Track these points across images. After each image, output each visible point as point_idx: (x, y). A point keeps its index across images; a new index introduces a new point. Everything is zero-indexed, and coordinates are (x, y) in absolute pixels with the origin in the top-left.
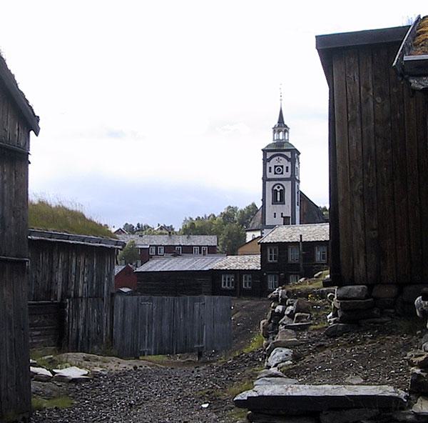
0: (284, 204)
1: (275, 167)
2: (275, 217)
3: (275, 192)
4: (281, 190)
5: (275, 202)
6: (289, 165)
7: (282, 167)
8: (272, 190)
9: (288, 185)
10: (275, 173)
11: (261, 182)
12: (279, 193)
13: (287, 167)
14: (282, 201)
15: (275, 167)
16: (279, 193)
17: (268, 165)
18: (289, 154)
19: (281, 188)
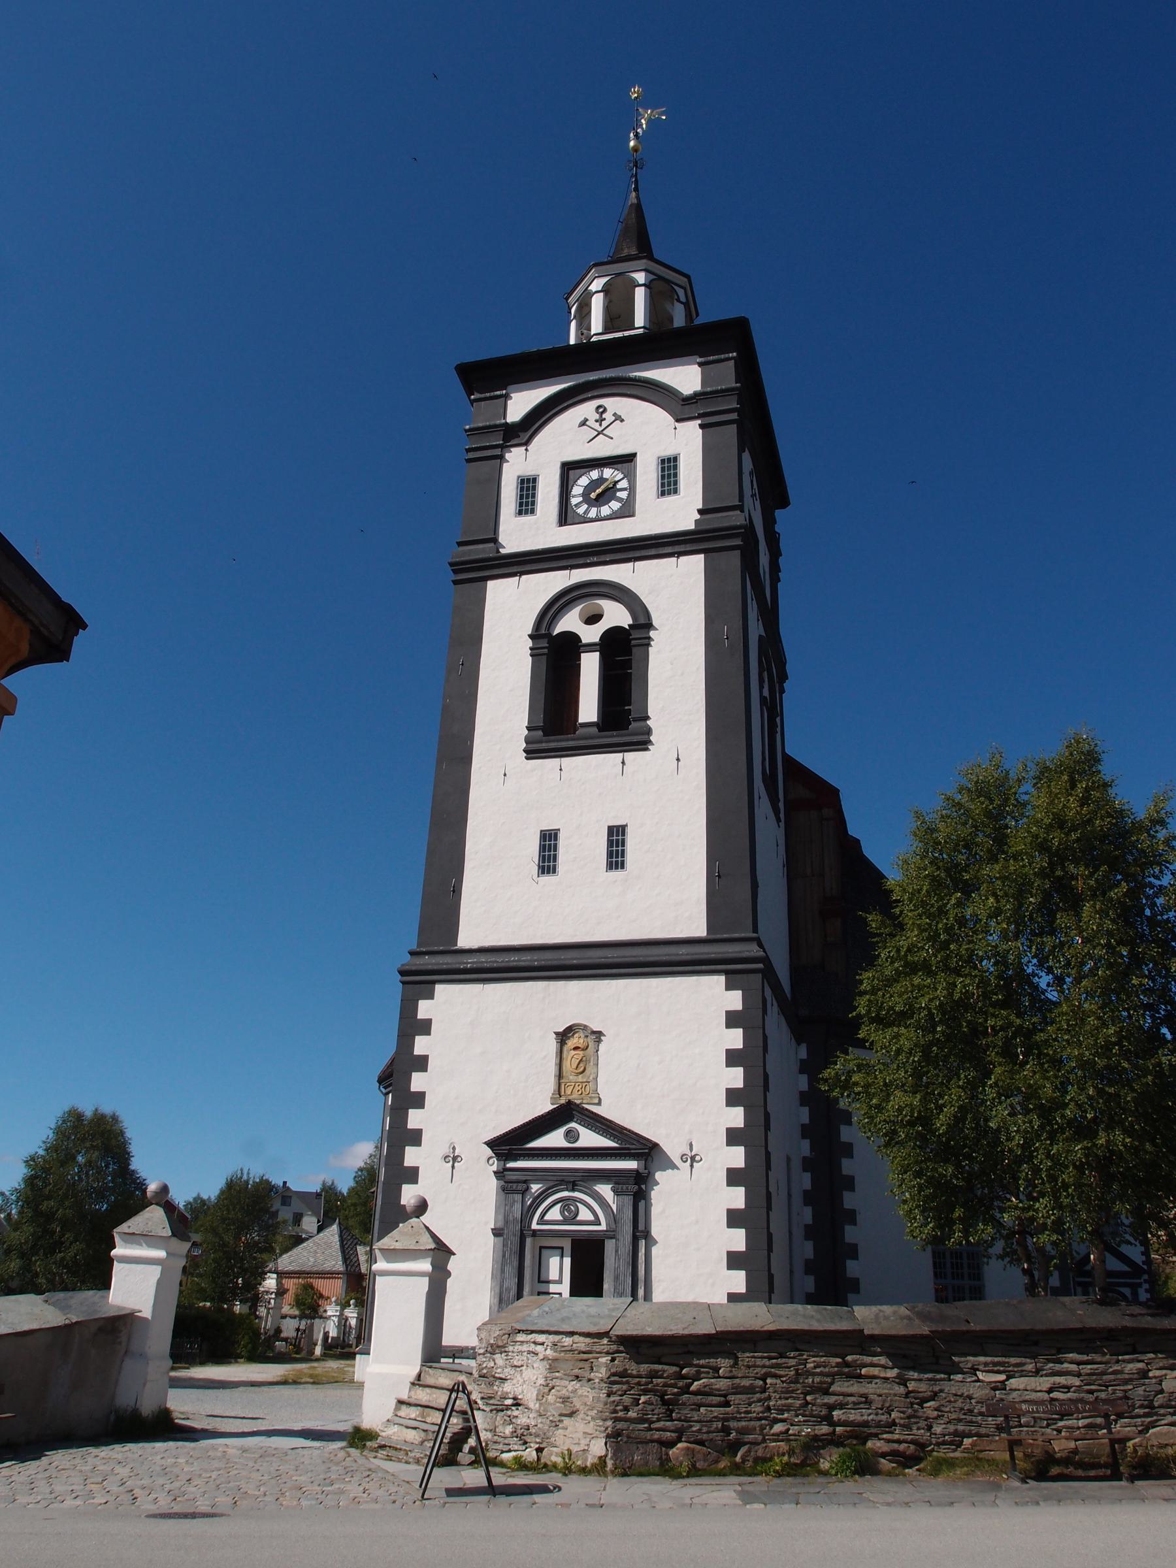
9: (676, 598)
10: (565, 517)
12: (590, 666)
13: (669, 468)
14: (623, 725)
15: (570, 469)
16: (590, 666)
18: (685, 377)
19: (616, 615)
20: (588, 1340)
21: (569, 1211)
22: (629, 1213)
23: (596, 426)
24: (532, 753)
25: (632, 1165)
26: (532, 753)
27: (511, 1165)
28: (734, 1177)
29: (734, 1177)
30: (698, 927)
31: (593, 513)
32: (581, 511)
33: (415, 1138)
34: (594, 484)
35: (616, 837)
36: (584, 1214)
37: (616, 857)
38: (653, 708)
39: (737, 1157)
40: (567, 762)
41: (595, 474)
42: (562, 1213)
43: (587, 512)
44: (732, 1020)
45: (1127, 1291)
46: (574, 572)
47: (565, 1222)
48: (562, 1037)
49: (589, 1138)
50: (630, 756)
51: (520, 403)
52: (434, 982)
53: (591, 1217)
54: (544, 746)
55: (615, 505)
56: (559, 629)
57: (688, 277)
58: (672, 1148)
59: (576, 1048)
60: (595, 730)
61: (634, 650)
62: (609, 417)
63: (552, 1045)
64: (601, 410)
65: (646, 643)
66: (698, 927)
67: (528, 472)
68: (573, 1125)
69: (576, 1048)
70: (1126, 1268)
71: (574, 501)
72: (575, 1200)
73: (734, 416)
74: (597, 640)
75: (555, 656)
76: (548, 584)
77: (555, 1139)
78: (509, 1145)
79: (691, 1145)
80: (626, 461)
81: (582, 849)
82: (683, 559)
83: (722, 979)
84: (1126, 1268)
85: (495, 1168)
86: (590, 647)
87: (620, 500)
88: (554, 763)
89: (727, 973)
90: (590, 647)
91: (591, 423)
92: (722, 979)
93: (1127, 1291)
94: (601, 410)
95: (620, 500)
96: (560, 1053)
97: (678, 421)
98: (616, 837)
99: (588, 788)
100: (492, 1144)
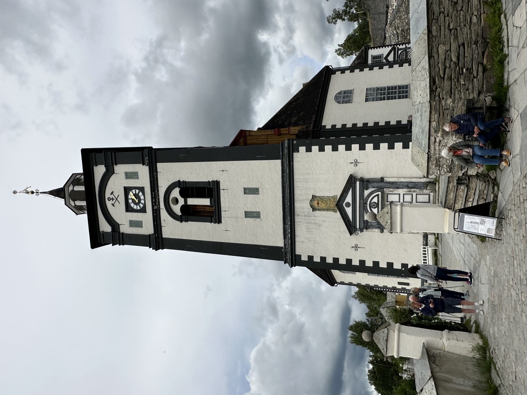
0: (217, 184)
1: (128, 209)
2: (248, 215)
4: (182, 194)
5: (213, 215)
6: (121, 169)
8: (180, 219)
10: (143, 210)
11: (166, 253)
12: (192, 201)
13: (129, 176)
14: (211, 190)
15: (128, 209)
16: (192, 201)
17: (125, 229)
18: (100, 171)
19: (176, 193)
20: (433, 113)
21: (374, 205)
22: (376, 184)
23: (114, 200)
24: (219, 221)
25: (358, 183)
26: (219, 221)
27: (358, 227)
28: (362, 148)
29: (362, 148)
30: (277, 163)
31: (143, 201)
32: (142, 206)
33: (349, 261)
34: (133, 201)
35: (248, 191)
36: (375, 200)
37: (254, 191)
38: (206, 180)
39: (355, 147)
40: (222, 209)
41: (130, 201)
42: (375, 208)
43: (142, 204)
44: (309, 150)
45: (400, 52)
46: (161, 207)
47: (378, 207)
48: (314, 209)
49: (349, 199)
50: (222, 187)
51: (105, 227)
52: (295, 255)
53: (376, 197)
54: (217, 217)
55: (141, 194)
56: (179, 213)
57: (73, 174)
58: (351, 170)
59: (318, 204)
60: (212, 199)
61: (187, 186)
62: (112, 196)
63: (317, 213)
64: (109, 199)
66: (277, 163)
67: (128, 224)
68: (344, 205)
69: (318, 204)
70: (393, 52)
71: (139, 208)
72: (370, 204)
73: (113, 153)
75: (189, 214)
77: (349, 211)
78: (351, 228)
79: (351, 163)
80: (127, 190)
81: (251, 203)
82: (158, 170)
83: (295, 154)
84: (393, 52)
85: (359, 232)
86: (186, 201)
87: (139, 192)
88: (223, 214)
89: (293, 152)
90: (186, 201)
91: (113, 202)
92: (295, 154)
93: (400, 52)
94: (109, 199)
95: (139, 192)
96: (320, 210)
97: (114, 173)
98: (248, 191)
99: (231, 201)
100: (351, 233)
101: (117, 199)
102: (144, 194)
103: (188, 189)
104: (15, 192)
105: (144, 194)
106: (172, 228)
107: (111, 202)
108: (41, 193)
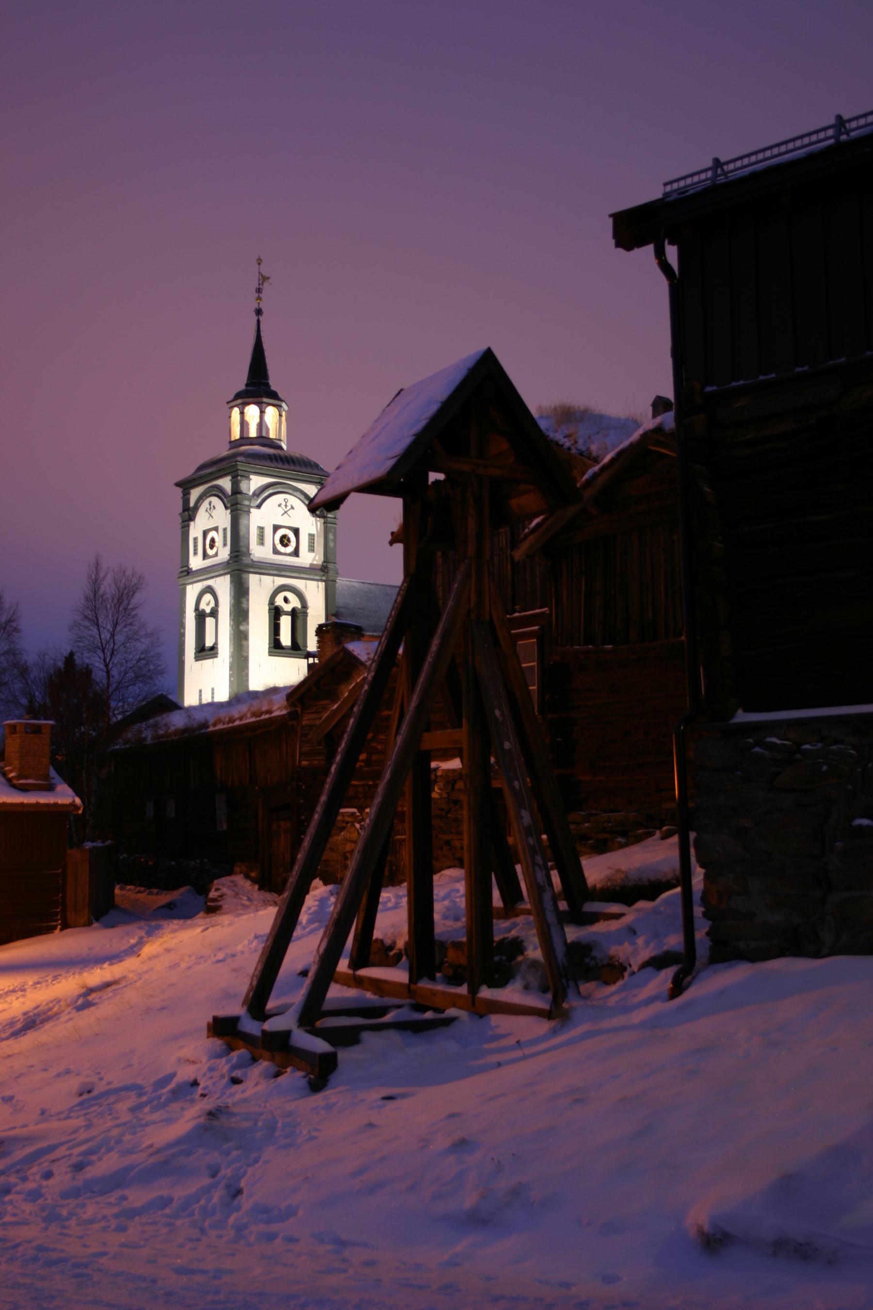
1: (276, 528)
3: (276, 613)
5: (276, 647)
7: (296, 532)
19: (295, 602)
65: (305, 614)
74: (290, 610)
76: (269, 583)
86: (287, 613)
101: (286, 512)
102: (289, 555)
103: (298, 616)
104: (259, 261)
105: (289, 555)
106: (260, 588)
107: (284, 503)
108: (258, 321)
